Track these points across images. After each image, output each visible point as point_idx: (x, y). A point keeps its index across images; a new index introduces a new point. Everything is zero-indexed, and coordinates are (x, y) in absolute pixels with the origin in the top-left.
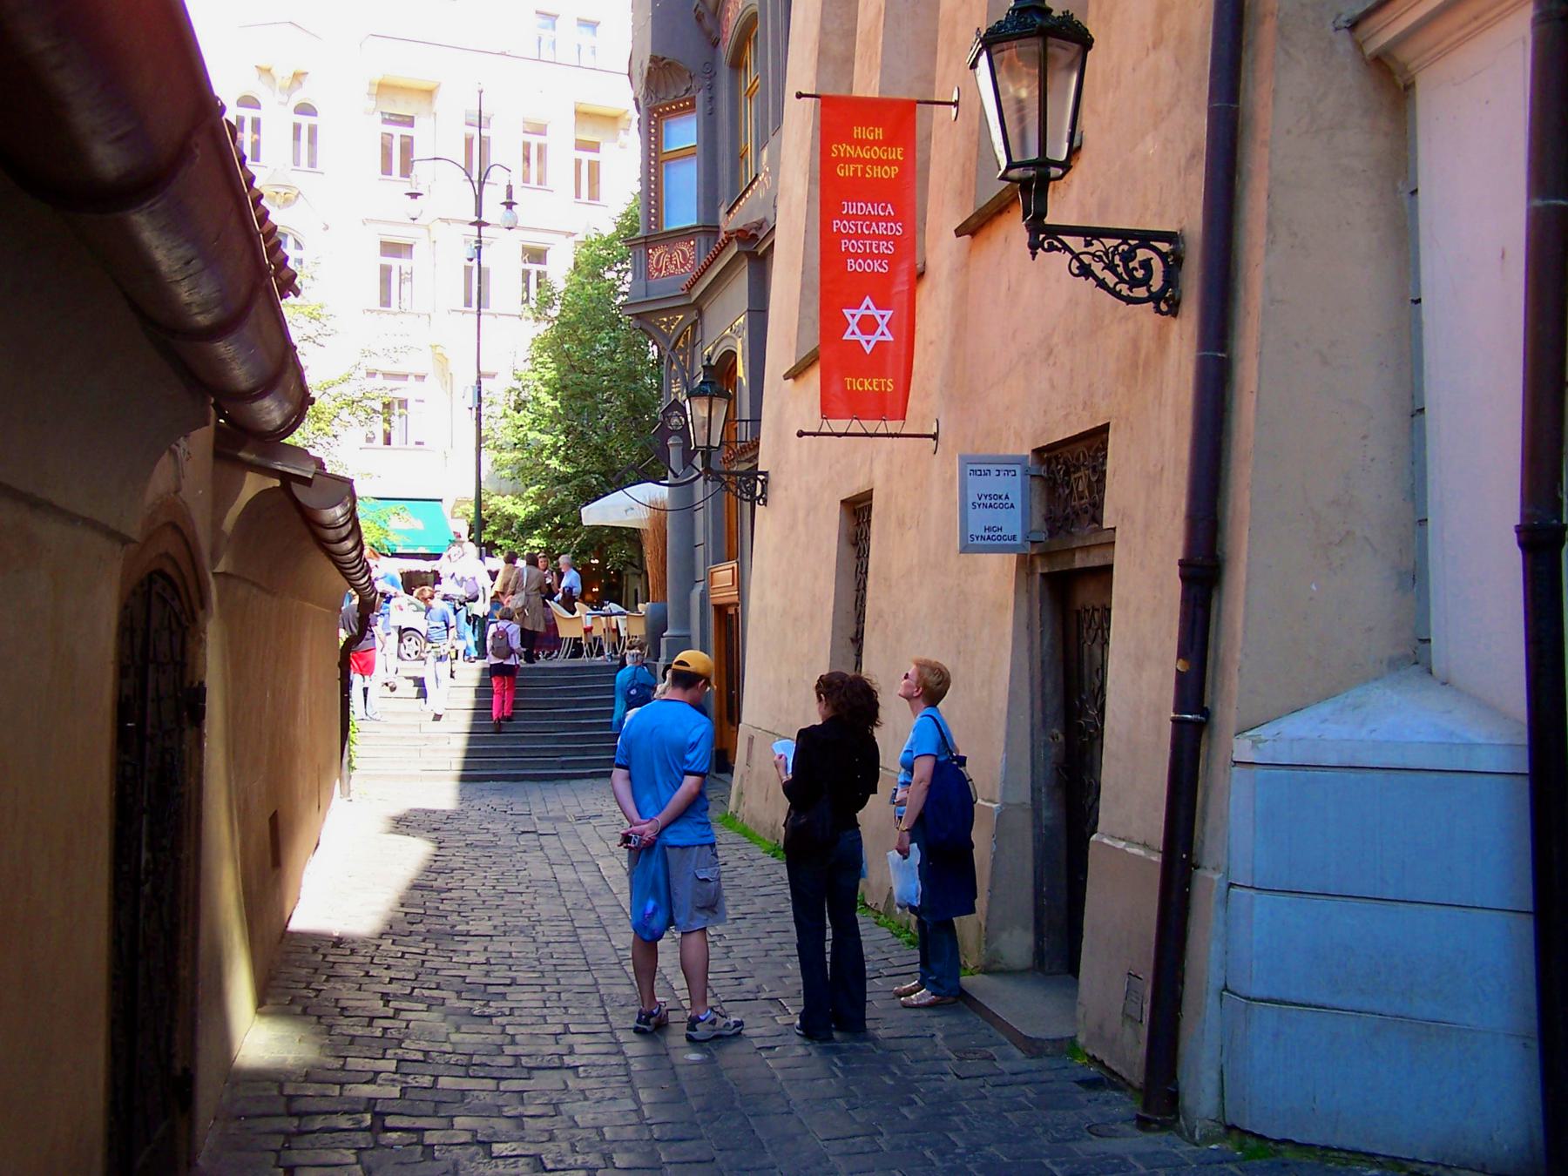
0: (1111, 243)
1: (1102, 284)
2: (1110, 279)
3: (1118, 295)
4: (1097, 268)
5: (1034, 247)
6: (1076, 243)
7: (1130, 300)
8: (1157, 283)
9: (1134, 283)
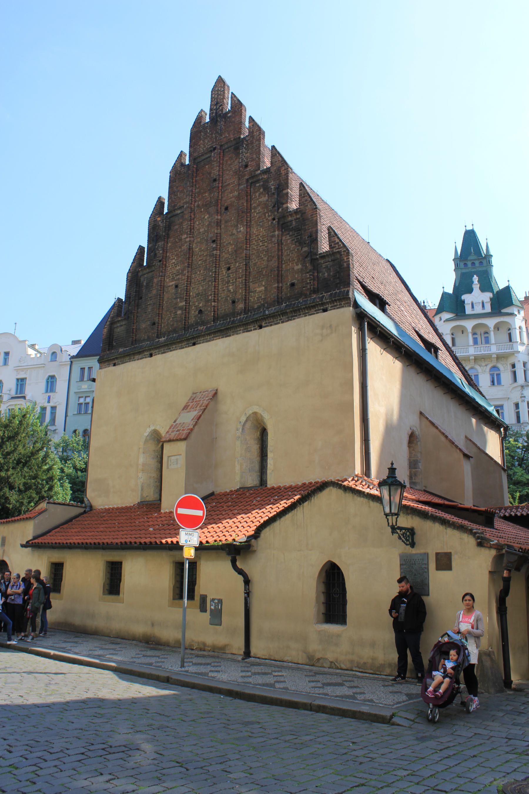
0: (404, 531)
1: (403, 541)
2: (404, 540)
3: (405, 543)
4: (402, 537)
5: (393, 533)
6: (398, 531)
7: (407, 545)
8: (410, 540)
9: (407, 540)
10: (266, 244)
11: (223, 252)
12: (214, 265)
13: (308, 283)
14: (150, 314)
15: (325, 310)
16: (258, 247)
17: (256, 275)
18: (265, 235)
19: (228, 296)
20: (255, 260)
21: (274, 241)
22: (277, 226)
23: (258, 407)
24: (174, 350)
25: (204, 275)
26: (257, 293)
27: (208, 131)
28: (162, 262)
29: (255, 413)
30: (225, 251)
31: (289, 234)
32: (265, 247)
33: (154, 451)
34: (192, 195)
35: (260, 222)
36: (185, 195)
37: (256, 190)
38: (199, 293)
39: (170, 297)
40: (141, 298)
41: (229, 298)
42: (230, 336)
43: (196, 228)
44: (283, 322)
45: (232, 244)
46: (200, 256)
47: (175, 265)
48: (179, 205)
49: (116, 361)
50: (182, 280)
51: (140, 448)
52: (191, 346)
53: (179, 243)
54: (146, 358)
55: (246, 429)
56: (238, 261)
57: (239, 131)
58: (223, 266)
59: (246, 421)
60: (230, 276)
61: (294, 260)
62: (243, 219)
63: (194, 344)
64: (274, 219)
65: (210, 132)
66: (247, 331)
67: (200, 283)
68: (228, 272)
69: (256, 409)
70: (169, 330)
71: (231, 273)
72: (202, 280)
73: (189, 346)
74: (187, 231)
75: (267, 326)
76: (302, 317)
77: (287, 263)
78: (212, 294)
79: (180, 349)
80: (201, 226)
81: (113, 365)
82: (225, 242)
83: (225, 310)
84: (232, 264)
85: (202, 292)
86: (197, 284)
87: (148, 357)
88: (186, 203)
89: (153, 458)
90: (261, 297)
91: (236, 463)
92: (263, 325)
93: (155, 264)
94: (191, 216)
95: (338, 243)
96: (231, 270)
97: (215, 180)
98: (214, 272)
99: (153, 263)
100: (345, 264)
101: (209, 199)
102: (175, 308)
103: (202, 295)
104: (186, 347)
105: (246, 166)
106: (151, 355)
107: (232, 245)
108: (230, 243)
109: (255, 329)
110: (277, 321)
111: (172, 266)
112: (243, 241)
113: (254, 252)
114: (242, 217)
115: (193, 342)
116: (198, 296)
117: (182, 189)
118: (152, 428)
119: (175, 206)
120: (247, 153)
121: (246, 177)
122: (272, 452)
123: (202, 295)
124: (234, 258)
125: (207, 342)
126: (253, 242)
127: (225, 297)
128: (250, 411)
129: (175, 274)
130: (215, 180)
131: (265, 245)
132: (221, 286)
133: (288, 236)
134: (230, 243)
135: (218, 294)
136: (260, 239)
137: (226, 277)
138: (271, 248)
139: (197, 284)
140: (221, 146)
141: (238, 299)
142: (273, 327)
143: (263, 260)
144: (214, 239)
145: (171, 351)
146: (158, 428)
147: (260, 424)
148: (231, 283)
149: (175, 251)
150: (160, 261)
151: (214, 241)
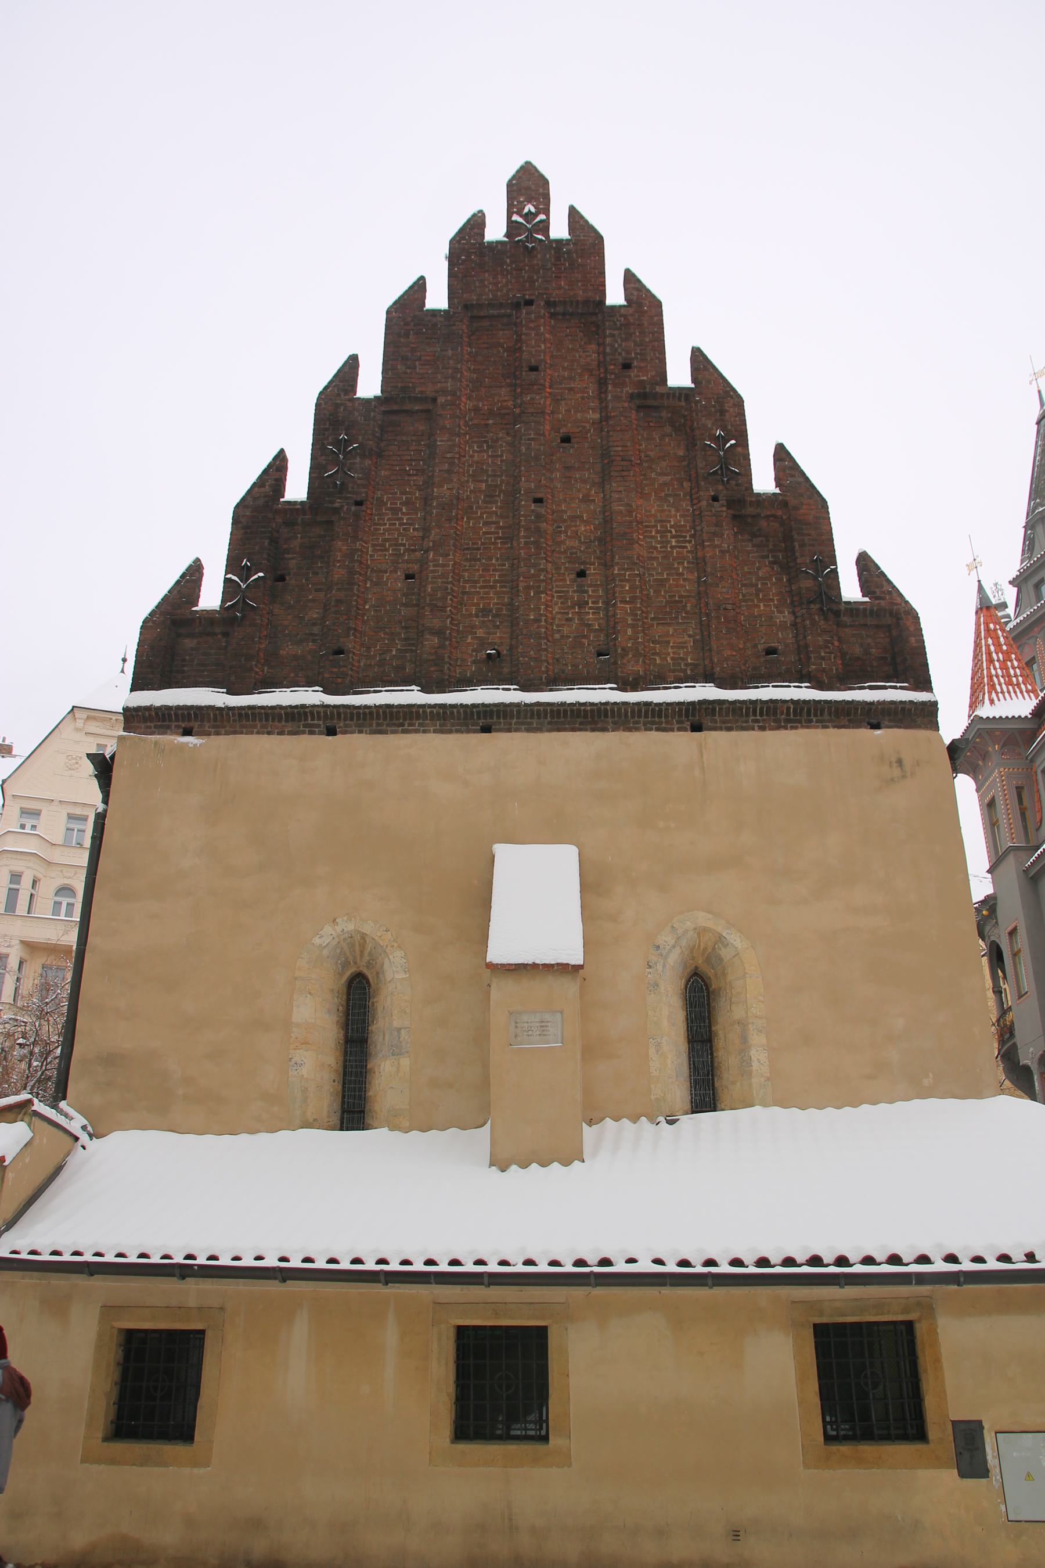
10: (687, 545)
11: (560, 532)
12: (543, 555)
13: (823, 658)
14: (314, 624)
15: (876, 726)
16: (666, 547)
17: (665, 606)
18: (685, 526)
19: (585, 637)
20: (658, 574)
21: (720, 546)
22: (724, 514)
23: (710, 916)
24: (416, 731)
25: (502, 570)
26: (672, 647)
27: (508, 261)
28: (364, 508)
29: (701, 931)
30: (566, 532)
31: (751, 541)
32: (688, 552)
33: (332, 991)
34: (461, 381)
35: (670, 495)
36: (439, 376)
37: (651, 424)
38: (491, 611)
39: (388, 599)
40: (282, 579)
41: (586, 641)
42: (604, 730)
43: (472, 456)
44: (762, 728)
45: (585, 521)
46: (486, 524)
47: (401, 524)
48: (421, 392)
49: (196, 725)
50: (435, 566)
51: (296, 979)
52: (475, 732)
53: (415, 478)
54: (311, 733)
55: (668, 966)
56: (618, 563)
57: (601, 288)
58: (564, 564)
59: (674, 947)
60: (587, 592)
61: (772, 600)
62: (624, 473)
63: (486, 729)
64: (715, 499)
65: (512, 262)
66: (657, 730)
67: (492, 587)
68: (579, 579)
69: (703, 919)
70: (385, 678)
71: (591, 586)
72: (496, 581)
73: (468, 731)
74: (449, 455)
75: (721, 729)
76: (817, 727)
77: (753, 601)
78: (540, 621)
79: (435, 732)
80: (489, 456)
81: (181, 730)
82: (565, 512)
83: (575, 666)
84: (592, 567)
85: (498, 610)
86: (482, 587)
87: (321, 733)
88: (444, 392)
89: (329, 1012)
90: (682, 659)
91: (652, 1051)
92: (707, 721)
93: (342, 507)
94: (459, 426)
95: (890, 593)
96: (589, 578)
97: (534, 369)
98: (542, 570)
99: (333, 502)
100: (913, 639)
101: (510, 403)
102: (406, 628)
103: (496, 616)
104: (458, 731)
105: (627, 366)
106: (331, 732)
107: (587, 523)
108: (581, 517)
109: (685, 730)
110: (747, 722)
111: (390, 524)
112: (631, 522)
113: (655, 554)
114: (623, 470)
115: (481, 722)
116: (483, 616)
117: (428, 358)
118: (350, 927)
119: (404, 389)
120: (626, 340)
121: (629, 389)
122: (761, 1031)
123: (496, 616)
124: (595, 551)
125: (528, 730)
126: (651, 532)
127: (575, 637)
128: (689, 923)
129: (404, 545)
130: (534, 369)
131: (686, 547)
132: (560, 608)
133: (750, 545)
134: (581, 517)
135: (552, 624)
136: (671, 532)
137: (574, 592)
138: (712, 557)
139: (482, 587)
140: (549, 304)
141: (623, 649)
142: (734, 733)
143: (685, 580)
144: (539, 495)
145: (404, 732)
146: (367, 929)
147: (693, 958)
148: (591, 608)
149: (402, 493)
150: (359, 503)
151: (538, 501)
